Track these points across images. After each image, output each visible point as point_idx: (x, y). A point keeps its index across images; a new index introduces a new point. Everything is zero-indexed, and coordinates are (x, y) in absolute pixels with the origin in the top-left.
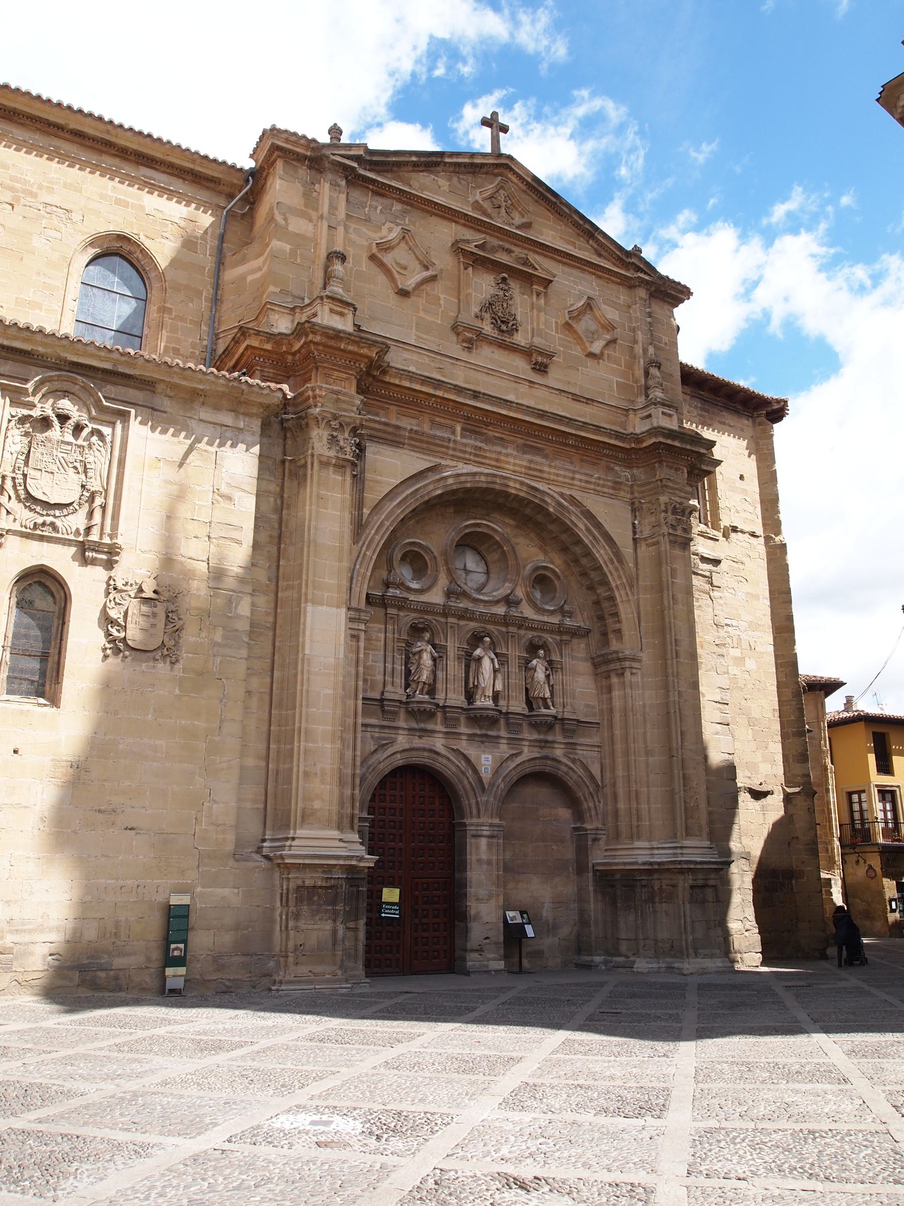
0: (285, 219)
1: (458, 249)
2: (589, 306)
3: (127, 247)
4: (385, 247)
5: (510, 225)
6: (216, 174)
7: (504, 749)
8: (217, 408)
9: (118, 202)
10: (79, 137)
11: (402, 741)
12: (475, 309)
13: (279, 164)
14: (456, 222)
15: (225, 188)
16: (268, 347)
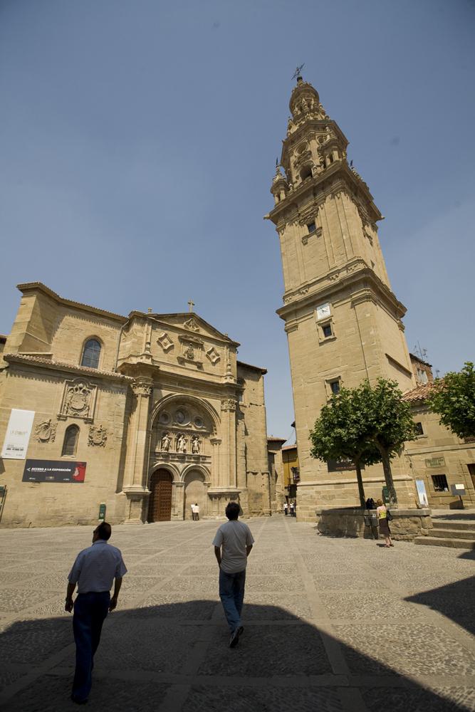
1: (180, 338)
2: (213, 350)
4: (161, 339)
7: (186, 464)
8: (117, 384)
9: (95, 327)
11: (160, 463)
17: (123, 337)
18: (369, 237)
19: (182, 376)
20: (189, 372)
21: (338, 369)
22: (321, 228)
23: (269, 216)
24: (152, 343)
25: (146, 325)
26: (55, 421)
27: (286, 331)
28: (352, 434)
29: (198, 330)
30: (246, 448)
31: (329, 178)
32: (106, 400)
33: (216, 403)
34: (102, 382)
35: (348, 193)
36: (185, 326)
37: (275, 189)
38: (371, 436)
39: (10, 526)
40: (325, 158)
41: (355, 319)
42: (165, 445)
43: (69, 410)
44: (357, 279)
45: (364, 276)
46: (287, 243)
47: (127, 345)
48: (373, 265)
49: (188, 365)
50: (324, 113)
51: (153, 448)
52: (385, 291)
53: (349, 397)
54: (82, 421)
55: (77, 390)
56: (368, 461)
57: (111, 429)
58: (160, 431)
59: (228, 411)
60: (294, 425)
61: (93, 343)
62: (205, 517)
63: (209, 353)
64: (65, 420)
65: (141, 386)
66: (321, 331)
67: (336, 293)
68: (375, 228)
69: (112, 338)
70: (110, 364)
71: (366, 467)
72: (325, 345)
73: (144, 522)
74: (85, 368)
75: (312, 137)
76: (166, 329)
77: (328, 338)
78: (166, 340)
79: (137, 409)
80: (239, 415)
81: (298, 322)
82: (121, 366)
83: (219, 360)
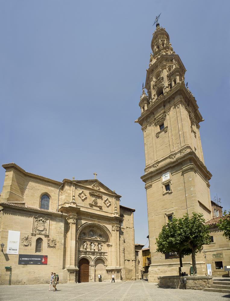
1: (90, 193)
2: (107, 199)
4: (80, 194)
8: (59, 217)
9: (45, 188)
17: (60, 193)
18: (195, 132)
19: (92, 213)
20: (95, 211)
21: (172, 209)
22: (167, 127)
23: (137, 120)
24: (75, 196)
25: (72, 186)
26: (30, 236)
27: (146, 188)
28: (178, 240)
29: (99, 189)
30: (124, 249)
31: (173, 95)
32: (54, 226)
33: (109, 227)
34: (51, 216)
35: (184, 104)
36: (92, 187)
37: (141, 104)
38: (187, 241)
39: (16, 284)
40: (171, 82)
41: (183, 182)
42: (85, 247)
43: (37, 231)
44: (186, 158)
45: (190, 156)
46: (148, 137)
47: (63, 197)
48: (195, 149)
49: (94, 208)
50: (172, 50)
51: (79, 248)
52: (201, 165)
53: (177, 222)
54: (44, 236)
55: (39, 221)
56: (186, 253)
57: (58, 240)
58: (82, 241)
59: (116, 231)
60: (148, 237)
61: (45, 197)
62: (105, 281)
63: (105, 201)
64: (35, 236)
65: (71, 218)
68: (198, 127)
69: (55, 194)
70: (55, 207)
71: (184, 256)
72: (166, 195)
73: (76, 283)
74: (42, 210)
75: (164, 67)
76: (83, 189)
78: (83, 195)
79: (70, 230)
80: (121, 233)
81: (152, 183)
82: (60, 209)
83: (110, 205)
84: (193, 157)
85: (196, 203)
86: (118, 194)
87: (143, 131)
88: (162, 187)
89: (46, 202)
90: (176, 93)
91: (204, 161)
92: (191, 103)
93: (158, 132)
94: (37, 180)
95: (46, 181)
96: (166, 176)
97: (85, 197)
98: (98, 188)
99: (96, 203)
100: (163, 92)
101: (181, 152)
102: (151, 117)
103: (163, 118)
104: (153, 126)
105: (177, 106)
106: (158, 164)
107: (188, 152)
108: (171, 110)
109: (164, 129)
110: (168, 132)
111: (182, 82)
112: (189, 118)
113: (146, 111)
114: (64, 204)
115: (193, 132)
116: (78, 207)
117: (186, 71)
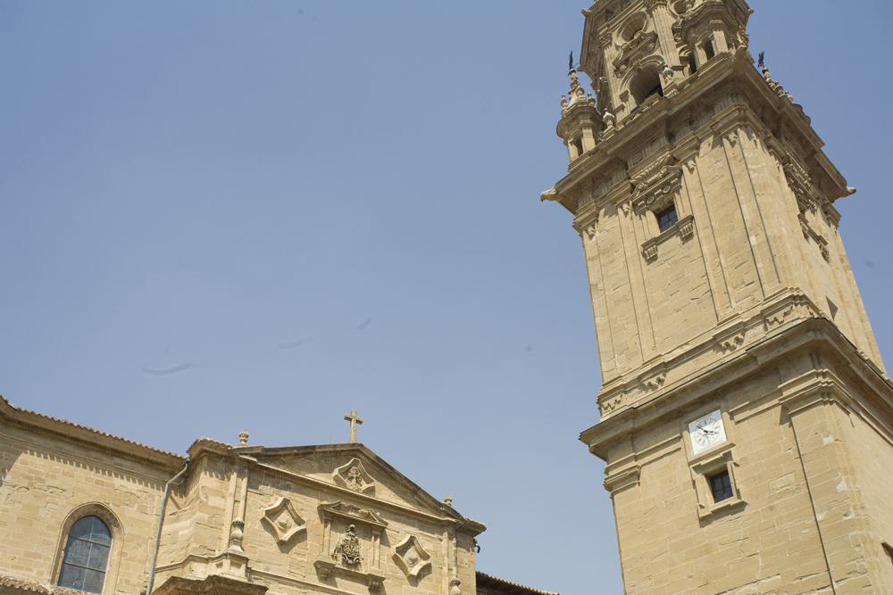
0: (206, 498)
1: (322, 511)
2: (411, 542)
3: (100, 511)
4: (272, 514)
5: (358, 491)
6: (163, 461)
9: (97, 482)
10: (76, 441)
12: (332, 551)
13: (205, 461)
14: (322, 491)
15: (169, 469)
16: (189, 588)
17: (171, 508)
18: (818, 239)
22: (692, 218)
23: (552, 191)
25: (234, 476)
27: (609, 487)
29: (371, 490)
31: (704, 95)
35: (757, 131)
36: (336, 478)
37: (568, 126)
40: (693, 48)
41: (793, 453)
44: (792, 346)
45: (811, 336)
46: (604, 259)
47: (184, 528)
48: (833, 309)
52: (871, 378)
63: (402, 550)
66: (701, 480)
67: (739, 384)
68: (832, 217)
69: (143, 511)
70: (134, 580)
72: (716, 523)
76: (287, 488)
77: (722, 504)
78: (284, 517)
81: (640, 463)
82: (163, 587)
83: (427, 569)
84: (826, 340)
85: (876, 554)
86: (469, 514)
87: (581, 236)
88: (694, 482)
89: (92, 553)
90: (717, 87)
91: (879, 356)
92: (788, 126)
93: (649, 238)
94: (61, 445)
95: (103, 450)
96: (706, 428)
97: (298, 528)
98: (365, 486)
99: (353, 560)
100: (660, 86)
101: (765, 321)
102: (614, 179)
103: (667, 183)
104: (626, 214)
105: (727, 138)
106: (661, 376)
107: (800, 321)
108: (702, 152)
109: (677, 228)
110: (695, 237)
111: (737, 52)
112: (786, 184)
113: (591, 153)
114: (183, 564)
115: (811, 239)
116: (257, 583)
117: (752, 12)
